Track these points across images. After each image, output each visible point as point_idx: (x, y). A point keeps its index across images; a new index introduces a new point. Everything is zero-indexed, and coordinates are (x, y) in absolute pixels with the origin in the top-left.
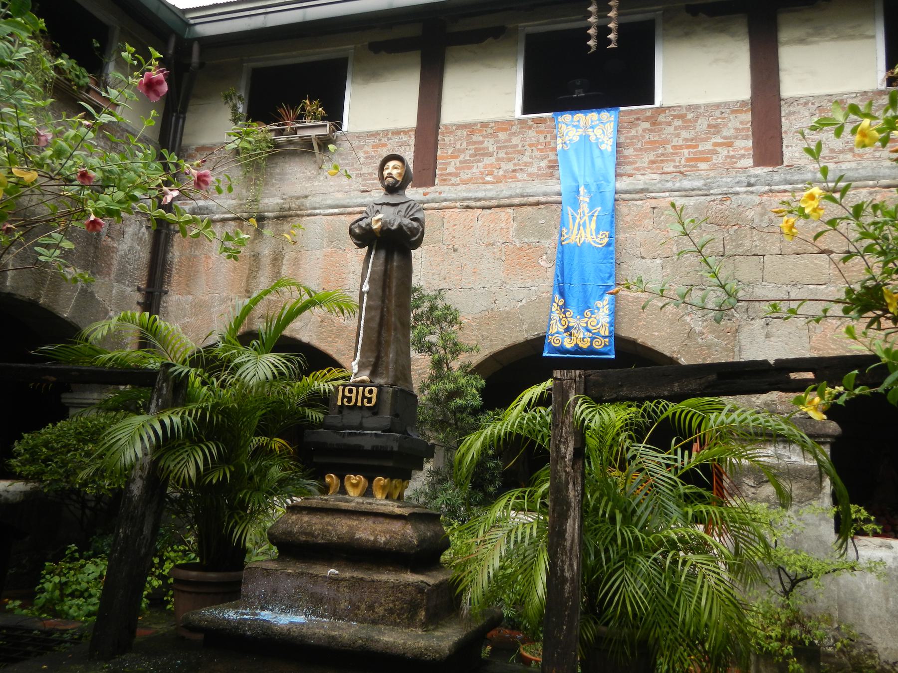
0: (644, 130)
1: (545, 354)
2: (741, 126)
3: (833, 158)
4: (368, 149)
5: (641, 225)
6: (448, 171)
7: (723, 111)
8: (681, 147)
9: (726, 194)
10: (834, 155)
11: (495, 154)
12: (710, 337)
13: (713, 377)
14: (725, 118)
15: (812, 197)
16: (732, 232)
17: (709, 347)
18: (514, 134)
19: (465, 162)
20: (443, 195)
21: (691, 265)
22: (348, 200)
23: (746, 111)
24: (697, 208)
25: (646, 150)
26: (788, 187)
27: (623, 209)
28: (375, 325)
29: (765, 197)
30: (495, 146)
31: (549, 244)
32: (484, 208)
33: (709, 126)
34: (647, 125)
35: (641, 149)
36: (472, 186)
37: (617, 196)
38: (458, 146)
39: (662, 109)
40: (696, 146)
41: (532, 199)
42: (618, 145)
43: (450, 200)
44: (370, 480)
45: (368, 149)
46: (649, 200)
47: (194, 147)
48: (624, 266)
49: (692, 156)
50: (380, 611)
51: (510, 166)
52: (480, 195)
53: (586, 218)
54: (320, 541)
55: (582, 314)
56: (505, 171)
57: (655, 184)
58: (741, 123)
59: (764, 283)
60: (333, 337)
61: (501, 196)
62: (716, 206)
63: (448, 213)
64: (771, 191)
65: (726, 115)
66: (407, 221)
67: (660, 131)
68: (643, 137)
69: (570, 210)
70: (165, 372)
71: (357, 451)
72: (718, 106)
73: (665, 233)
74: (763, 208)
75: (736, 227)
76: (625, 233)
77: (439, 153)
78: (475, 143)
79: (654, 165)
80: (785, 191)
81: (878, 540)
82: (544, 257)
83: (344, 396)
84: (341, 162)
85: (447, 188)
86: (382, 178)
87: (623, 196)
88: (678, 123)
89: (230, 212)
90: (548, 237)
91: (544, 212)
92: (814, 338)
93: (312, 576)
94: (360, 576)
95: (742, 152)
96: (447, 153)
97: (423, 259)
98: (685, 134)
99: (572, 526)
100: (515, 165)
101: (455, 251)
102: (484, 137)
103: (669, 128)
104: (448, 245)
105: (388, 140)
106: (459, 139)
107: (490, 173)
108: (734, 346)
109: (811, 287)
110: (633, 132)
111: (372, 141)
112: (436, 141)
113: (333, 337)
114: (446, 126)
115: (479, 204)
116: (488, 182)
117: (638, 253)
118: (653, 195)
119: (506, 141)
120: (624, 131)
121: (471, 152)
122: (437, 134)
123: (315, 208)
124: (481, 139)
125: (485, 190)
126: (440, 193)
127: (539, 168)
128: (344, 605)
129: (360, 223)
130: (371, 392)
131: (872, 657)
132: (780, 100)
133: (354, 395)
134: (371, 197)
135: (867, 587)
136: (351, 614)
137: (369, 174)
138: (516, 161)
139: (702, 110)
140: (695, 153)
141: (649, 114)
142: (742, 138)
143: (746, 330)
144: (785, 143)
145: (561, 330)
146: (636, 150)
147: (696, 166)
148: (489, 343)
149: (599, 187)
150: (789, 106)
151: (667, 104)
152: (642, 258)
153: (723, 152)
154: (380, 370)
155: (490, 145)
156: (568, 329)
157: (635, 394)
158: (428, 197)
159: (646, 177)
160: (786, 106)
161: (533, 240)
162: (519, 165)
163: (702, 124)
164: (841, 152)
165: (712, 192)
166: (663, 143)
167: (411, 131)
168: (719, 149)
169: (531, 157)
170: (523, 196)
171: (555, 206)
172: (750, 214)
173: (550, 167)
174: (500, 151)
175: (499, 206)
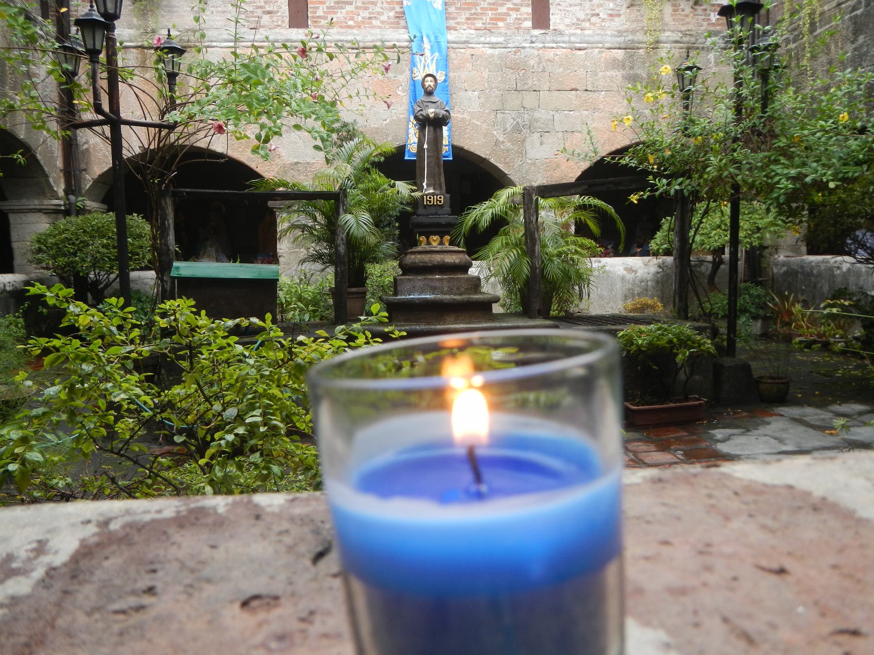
1: (406, 158)
3: (579, 25)
6: (317, 15)
8: (486, 9)
12: (509, 144)
15: (628, 119)
16: (521, 75)
17: (508, 151)
19: (331, 7)
21: (496, 96)
24: (500, 57)
25: (464, 9)
26: (554, 45)
29: (541, 51)
40: (497, 9)
44: (442, 237)
48: (454, 96)
49: (493, 16)
50: (462, 289)
51: (366, 14)
52: (350, 38)
53: (429, 61)
54: (429, 265)
56: (363, 18)
57: (473, 38)
61: (366, 40)
66: (445, 113)
71: (438, 225)
74: (540, 59)
75: (523, 71)
76: (454, 72)
80: (553, 48)
82: (400, 88)
83: (427, 200)
87: (452, 45)
89: (131, 41)
90: (402, 73)
93: (430, 279)
95: (525, 16)
100: (370, 13)
107: (352, 19)
108: (522, 150)
123: (212, 41)
127: (389, 18)
128: (446, 289)
129: (421, 112)
130: (440, 198)
136: (450, 292)
138: (371, 10)
140: (496, 14)
143: (529, 140)
147: (496, 24)
149: (436, 38)
153: (514, 15)
154: (436, 186)
157: (557, 194)
159: (466, 31)
162: (373, 13)
164: (583, 21)
165: (509, 45)
168: (511, 13)
169: (382, 8)
172: (532, 62)
173: (397, 17)
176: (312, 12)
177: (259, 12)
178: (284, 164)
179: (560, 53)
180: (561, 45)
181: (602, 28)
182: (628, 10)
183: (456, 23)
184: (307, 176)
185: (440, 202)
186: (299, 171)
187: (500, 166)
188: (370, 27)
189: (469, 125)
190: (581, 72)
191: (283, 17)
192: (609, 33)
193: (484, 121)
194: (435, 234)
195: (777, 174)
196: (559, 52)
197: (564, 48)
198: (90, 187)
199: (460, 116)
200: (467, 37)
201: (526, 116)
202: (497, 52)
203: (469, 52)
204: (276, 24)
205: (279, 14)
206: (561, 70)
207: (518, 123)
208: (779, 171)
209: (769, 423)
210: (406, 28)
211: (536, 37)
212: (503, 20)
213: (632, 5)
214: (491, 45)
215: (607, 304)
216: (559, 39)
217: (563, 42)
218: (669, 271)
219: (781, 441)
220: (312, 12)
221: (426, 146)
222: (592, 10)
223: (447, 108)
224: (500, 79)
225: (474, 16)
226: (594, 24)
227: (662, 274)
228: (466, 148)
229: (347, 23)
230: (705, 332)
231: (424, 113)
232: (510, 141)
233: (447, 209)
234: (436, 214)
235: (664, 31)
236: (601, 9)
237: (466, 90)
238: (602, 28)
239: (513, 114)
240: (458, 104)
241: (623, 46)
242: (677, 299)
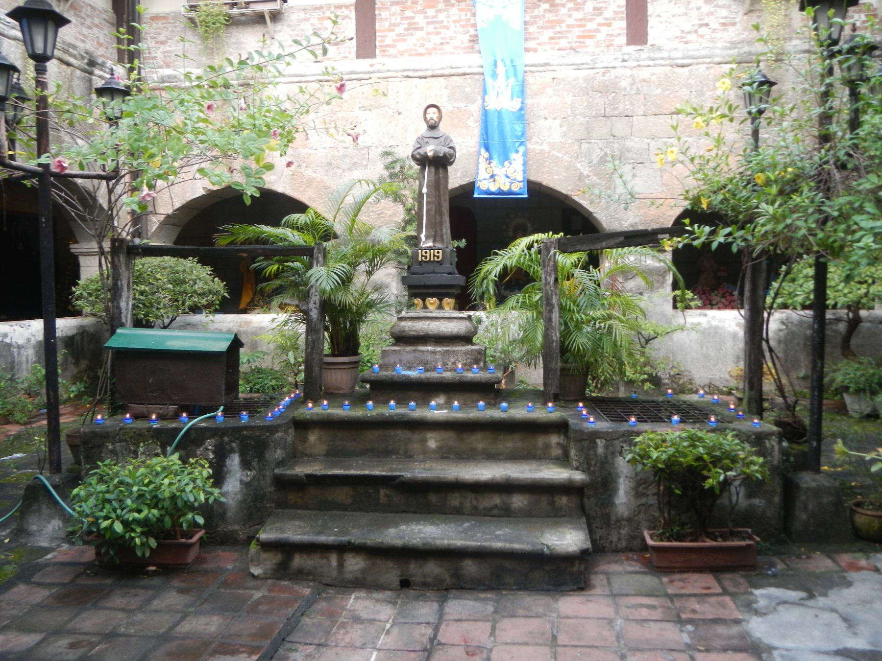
0: (545, 11)
1: (476, 195)
3: (683, 37)
6: (386, 43)
10: (684, 35)
12: (595, 178)
13: (622, 239)
15: (672, 152)
18: (439, 11)
19: (400, 35)
20: (386, 68)
21: (581, 124)
24: (586, 80)
25: (547, 28)
26: (651, 63)
27: (530, 79)
28: (433, 213)
29: (635, 71)
30: (425, 21)
31: (475, 108)
32: (421, 78)
33: (595, 9)
35: (542, 28)
37: (527, 69)
40: (584, 26)
41: (460, 71)
42: (526, 23)
44: (441, 300)
47: (148, 16)
48: (532, 125)
49: (581, 34)
51: (437, 39)
55: (502, 164)
56: (435, 44)
62: (599, 78)
64: (639, 66)
66: (446, 150)
68: (544, 16)
69: (489, 81)
70: (318, 249)
74: (633, 79)
75: (613, 95)
78: (407, 18)
79: (553, 41)
80: (649, 66)
81: (699, 311)
82: (472, 118)
83: (422, 256)
86: (425, 119)
90: (474, 101)
91: (469, 81)
92: (665, 177)
93: (420, 351)
94: (447, 349)
98: (577, 15)
99: (556, 315)
100: (442, 38)
101: (399, 113)
106: (394, 14)
107: (422, 45)
109: (664, 140)
110: (536, 13)
111: (316, 14)
119: (436, 17)
120: (529, 10)
122: (374, 9)
124: (412, 14)
129: (419, 150)
131: (691, 384)
133: (428, 255)
135: (691, 341)
138: (442, 35)
140: (584, 31)
144: (650, 24)
145: (488, 176)
146: (539, 27)
149: (512, 61)
152: (546, 118)
153: (604, 29)
154: (437, 238)
155: (420, 19)
156: (492, 176)
161: (462, 105)
164: (689, 33)
165: (596, 66)
166: (560, 22)
168: (601, 28)
170: (452, 68)
171: (477, 77)
173: (471, 41)
175: (433, 76)
181: (712, 40)
182: (745, 17)
185: (438, 257)
187: (585, 203)
188: (442, 54)
190: (685, 92)
192: (719, 45)
193: (567, 153)
194: (432, 295)
195: (861, 229)
196: (658, 70)
198: (157, 229)
199: (538, 147)
201: (616, 145)
204: (342, 55)
206: (659, 91)
208: (863, 224)
209: (849, 584)
210: (479, 52)
211: (629, 54)
213: (751, 11)
215: (714, 365)
216: (658, 55)
217: (662, 59)
218: (794, 329)
219: (849, 622)
221: (425, 190)
222: (701, 20)
223: (451, 145)
224: (585, 104)
225: (559, 35)
226: (702, 36)
227: (786, 331)
228: (544, 183)
229: (416, 50)
230: (769, 440)
231: (421, 151)
232: (596, 175)
233: (447, 266)
234: (433, 272)
235: (791, 39)
236: (711, 18)
238: (712, 40)
239: (601, 144)
241: (738, 59)
242: (747, 386)
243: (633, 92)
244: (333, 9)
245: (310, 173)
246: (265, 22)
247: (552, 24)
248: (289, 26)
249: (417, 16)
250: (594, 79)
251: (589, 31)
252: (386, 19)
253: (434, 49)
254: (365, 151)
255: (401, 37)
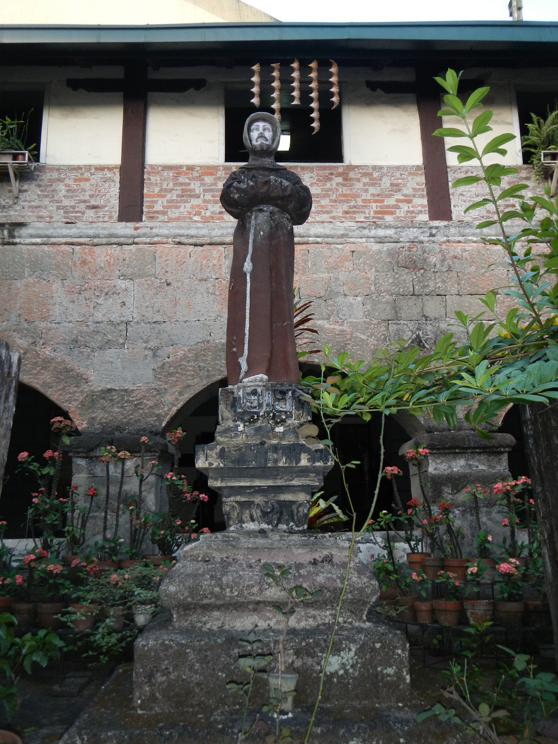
0: (338, 184)
2: (418, 187)
4: (71, 182)
5: (343, 266)
6: (155, 209)
7: (402, 173)
8: (369, 201)
9: (413, 242)
10: (490, 215)
11: (202, 196)
14: (403, 179)
19: (172, 201)
20: (155, 231)
21: (387, 302)
22: (52, 231)
23: (421, 174)
24: (390, 253)
25: (340, 201)
26: (461, 238)
29: (444, 247)
30: (202, 189)
32: (196, 245)
33: (392, 185)
34: (340, 180)
36: (183, 224)
38: (165, 186)
39: (352, 168)
40: (382, 201)
43: (162, 236)
45: (71, 182)
46: (348, 245)
49: (379, 209)
52: (192, 232)
56: (212, 213)
57: (354, 231)
58: (418, 184)
59: (447, 319)
60: (38, 369)
61: (213, 234)
63: (159, 247)
65: (405, 177)
67: (351, 186)
68: (337, 190)
72: (398, 168)
73: (364, 274)
74: (443, 255)
75: (422, 271)
77: (145, 191)
78: (181, 184)
79: (348, 215)
80: (459, 242)
84: (39, 193)
85: (157, 224)
88: (366, 180)
95: (420, 208)
96: (153, 192)
97: (136, 292)
98: (372, 190)
101: (168, 284)
102: (190, 179)
103: (358, 184)
104: (161, 279)
105: (92, 174)
106: (165, 180)
107: (198, 214)
110: (328, 185)
111: (73, 175)
112: (143, 180)
113: (38, 369)
114: (152, 167)
115: (191, 241)
116: (196, 222)
117: (341, 291)
118: (352, 240)
119: (212, 184)
121: (177, 192)
124: (187, 181)
125: (197, 228)
126: (151, 228)
132: (447, 167)
134: (78, 228)
137: (71, 206)
139: (385, 171)
140: (381, 207)
141: (341, 170)
142: (419, 197)
146: (331, 201)
147: (383, 218)
148: (206, 373)
150: (454, 173)
151: (355, 163)
153: (405, 207)
155: (196, 186)
158: (138, 231)
160: (451, 173)
163: (386, 183)
165: (401, 240)
167: (116, 168)
168: (400, 204)
174: (206, 194)
175: (211, 244)
176: (148, 207)
177: (82, 206)
178: (92, 391)
179: (470, 248)
180: (470, 238)
183: (331, 218)
184: (122, 407)
186: (112, 400)
189: (350, 339)
191: (111, 212)
193: (372, 334)
196: (469, 247)
197: (475, 242)
200: (346, 229)
201: (429, 328)
202: (386, 247)
203: (348, 248)
205: (107, 209)
206: (473, 269)
207: (418, 336)
211: (437, 228)
212: (391, 213)
214: (378, 240)
216: (467, 231)
220: (148, 207)
221: (248, 266)
224: (391, 281)
225: (354, 209)
229: (191, 219)
237: (345, 295)
240: (335, 313)
243: (445, 270)
244: (93, 170)
245: (48, 352)
246: (9, 180)
247: (346, 198)
248: (39, 186)
249: (192, 182)
250: (398, 253)
251: (388, 206)
252: (156, 184)
253: (212, 218)
254: (122, 327)
255: (173, 204)
